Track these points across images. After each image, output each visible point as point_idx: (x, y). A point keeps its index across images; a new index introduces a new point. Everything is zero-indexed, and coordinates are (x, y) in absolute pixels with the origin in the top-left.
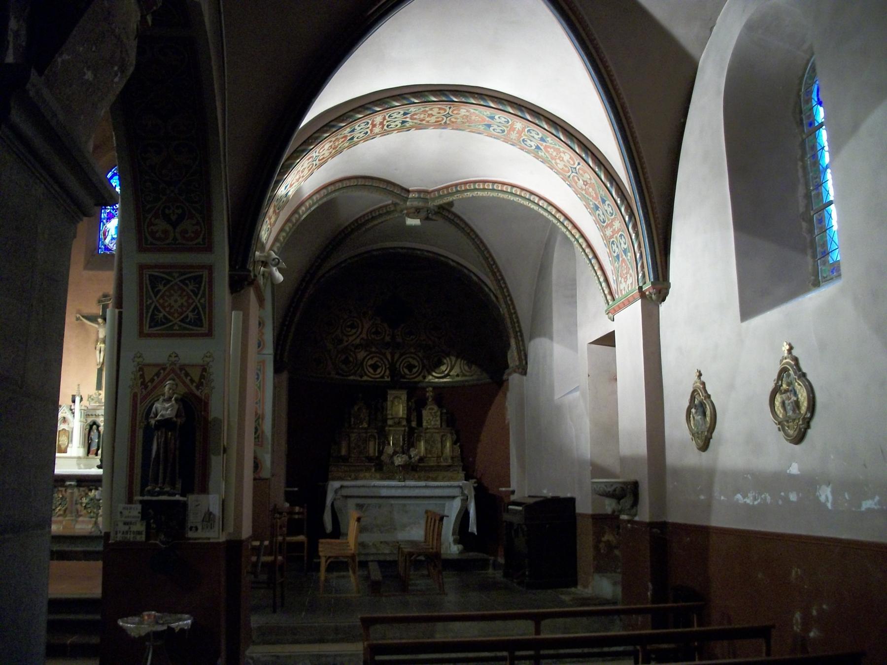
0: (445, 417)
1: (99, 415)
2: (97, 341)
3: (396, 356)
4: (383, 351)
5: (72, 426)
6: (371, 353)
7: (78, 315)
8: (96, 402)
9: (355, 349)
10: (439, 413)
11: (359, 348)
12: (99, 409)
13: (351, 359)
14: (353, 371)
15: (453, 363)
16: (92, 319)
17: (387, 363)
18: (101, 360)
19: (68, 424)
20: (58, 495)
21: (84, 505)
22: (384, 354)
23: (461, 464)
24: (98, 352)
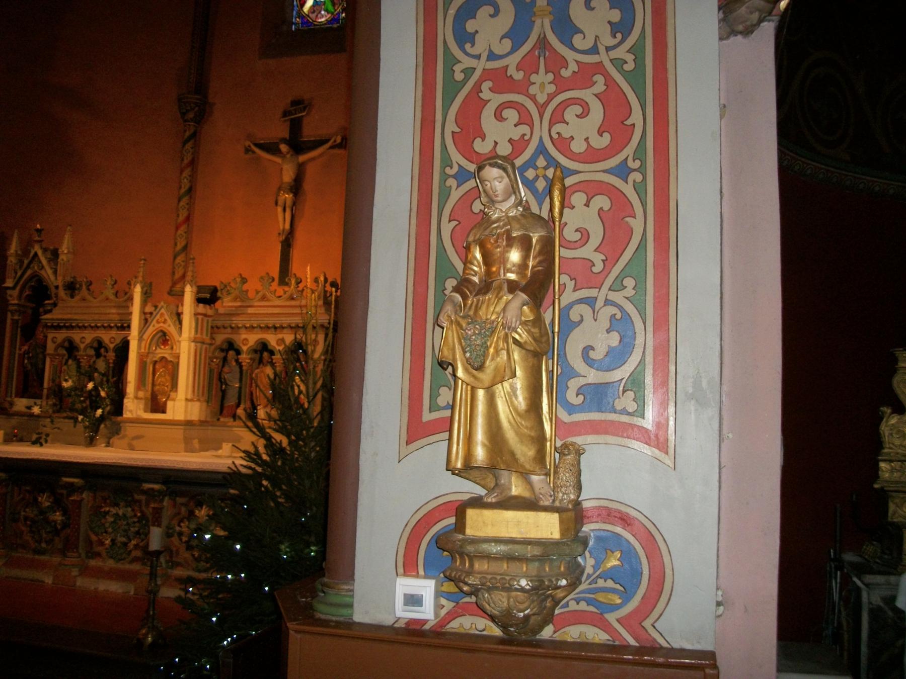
1: (238, 328)
2: (280, 189)
5: (178, 351)
7: (248, 143)
8: (235, 299)
12: (238, 314)
16: (271, 148)
18: (287, 226)
19: (172, 348)
20: (133, 510)
21: (184, 539)
24: (280, 209)
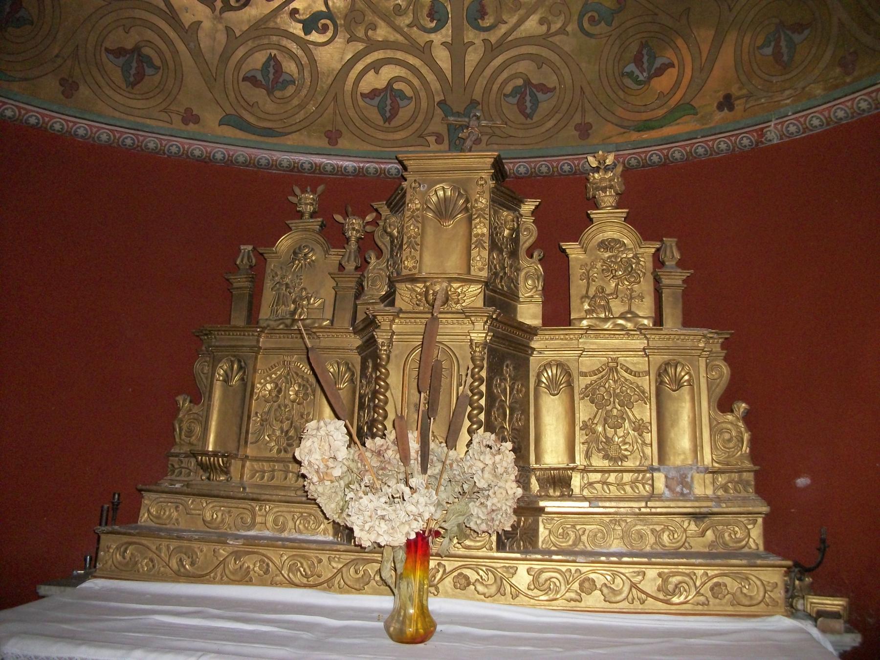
0: (675, 278)
3: (472, 58)
4: (422, 38)
6: (372, 46)
9: (307, 31)
10: (646, 262)
11: (325, 28)
13: (290, 67)
14: (301, 115)
15: (705, 48)
17: (435, 85)
22: (424, 51)
23: (765, 509)
